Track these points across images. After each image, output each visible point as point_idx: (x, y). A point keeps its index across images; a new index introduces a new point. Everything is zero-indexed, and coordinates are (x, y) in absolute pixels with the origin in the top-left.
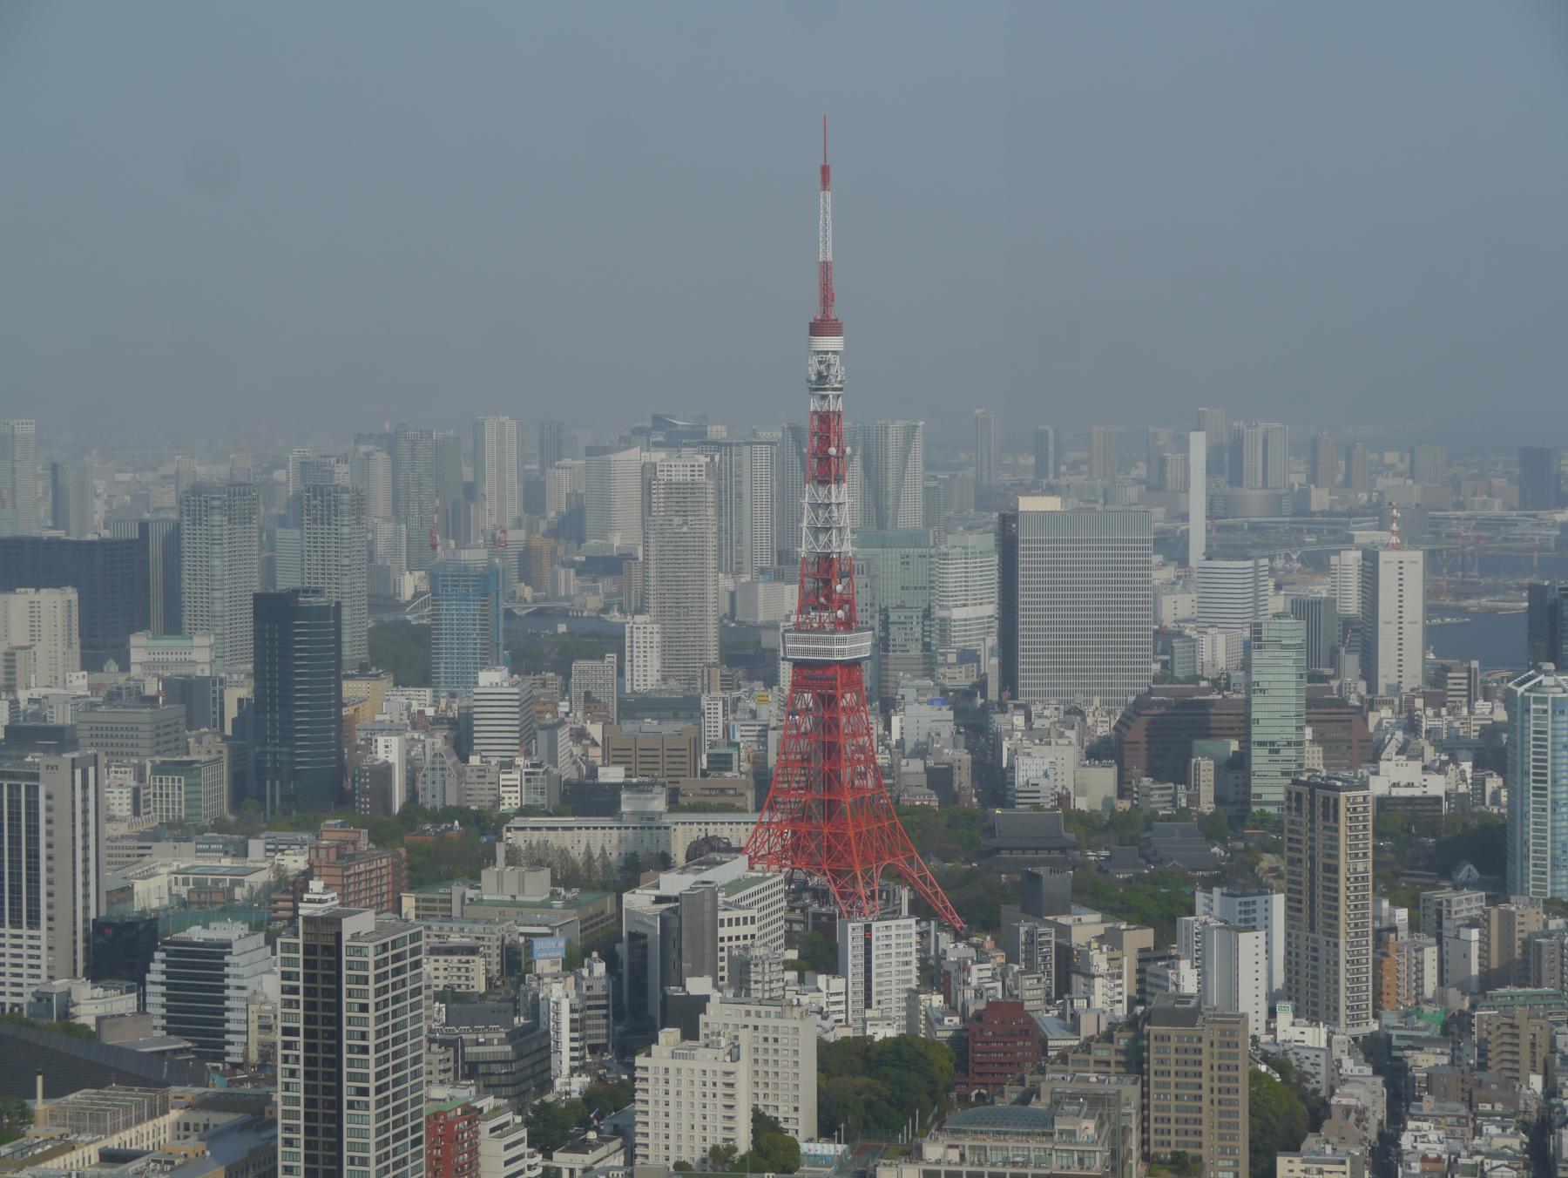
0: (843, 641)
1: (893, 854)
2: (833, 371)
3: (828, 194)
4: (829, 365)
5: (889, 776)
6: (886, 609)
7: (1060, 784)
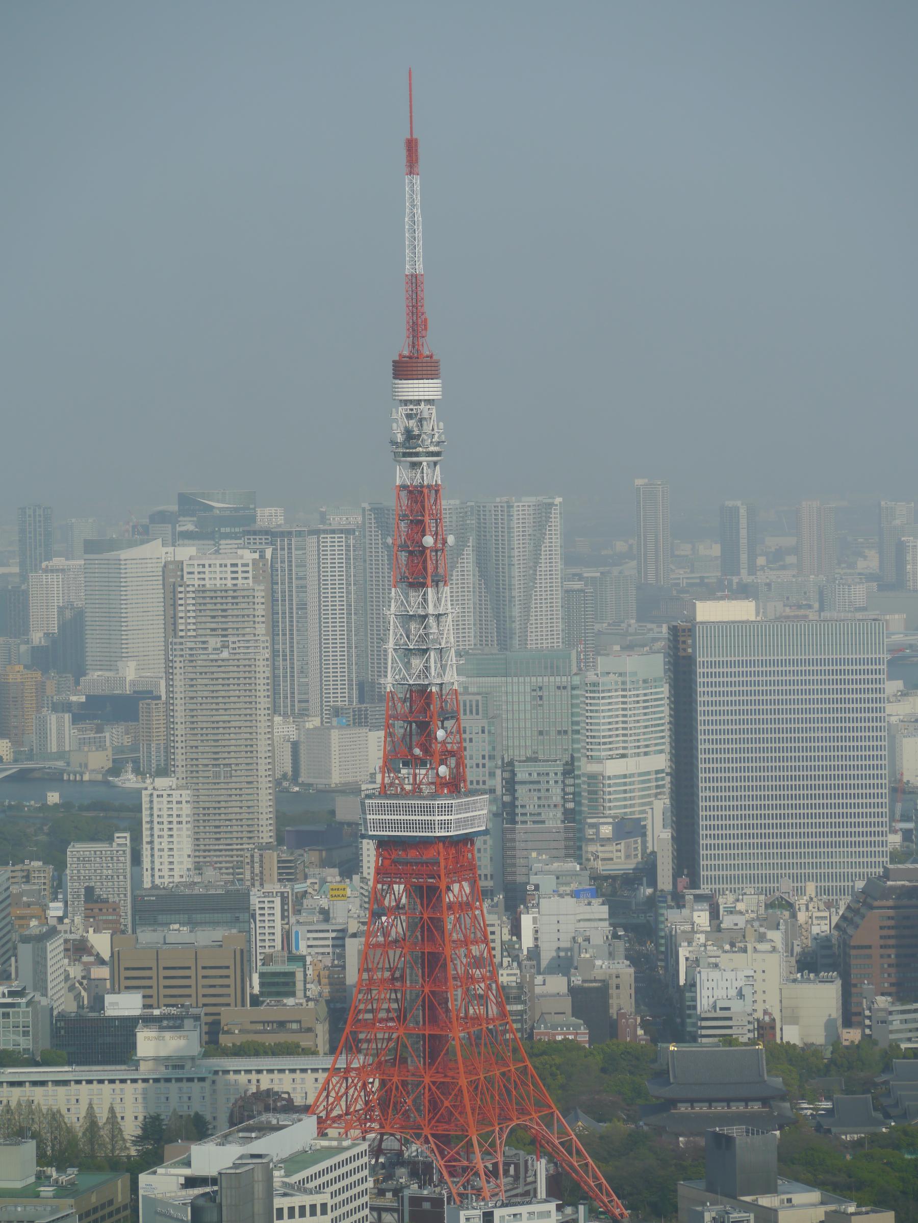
0: (448, 809)
1: (523, 1112)
2: (427, 428)
3: (417, 180)
4: (421, 420)
5: (518, 1000)
6: (511, 763)
7: (760, 1007)
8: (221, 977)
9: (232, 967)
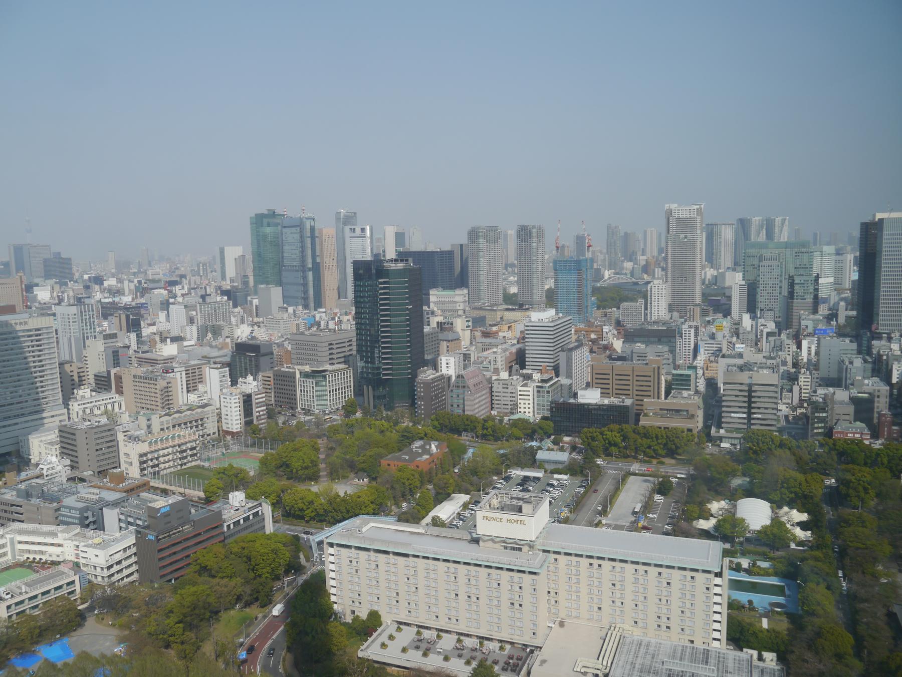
5: (823, 410)
6: (792, 276)
8: (647, 381)
9: (652, 377)
